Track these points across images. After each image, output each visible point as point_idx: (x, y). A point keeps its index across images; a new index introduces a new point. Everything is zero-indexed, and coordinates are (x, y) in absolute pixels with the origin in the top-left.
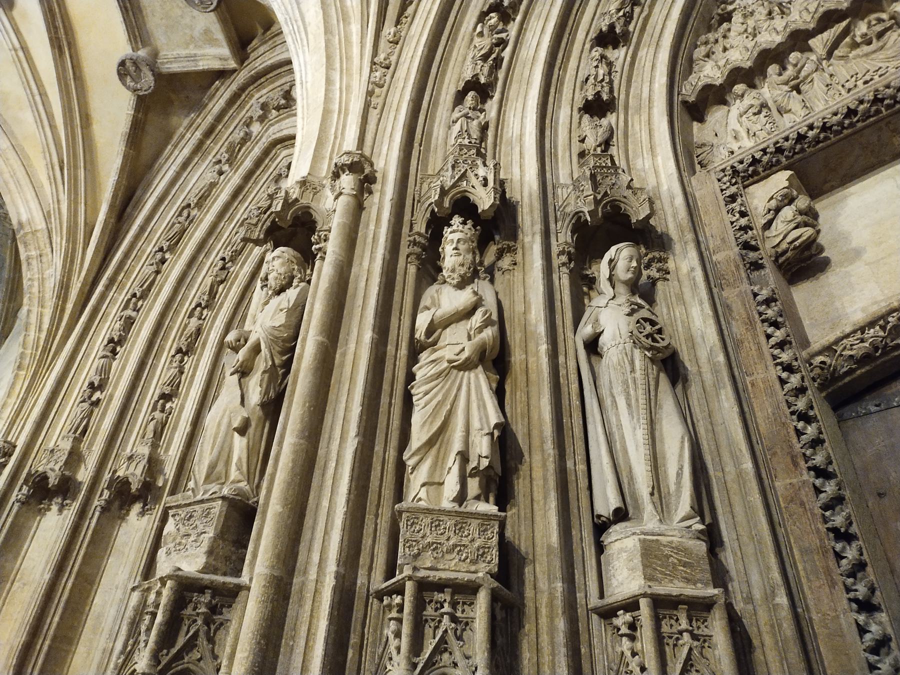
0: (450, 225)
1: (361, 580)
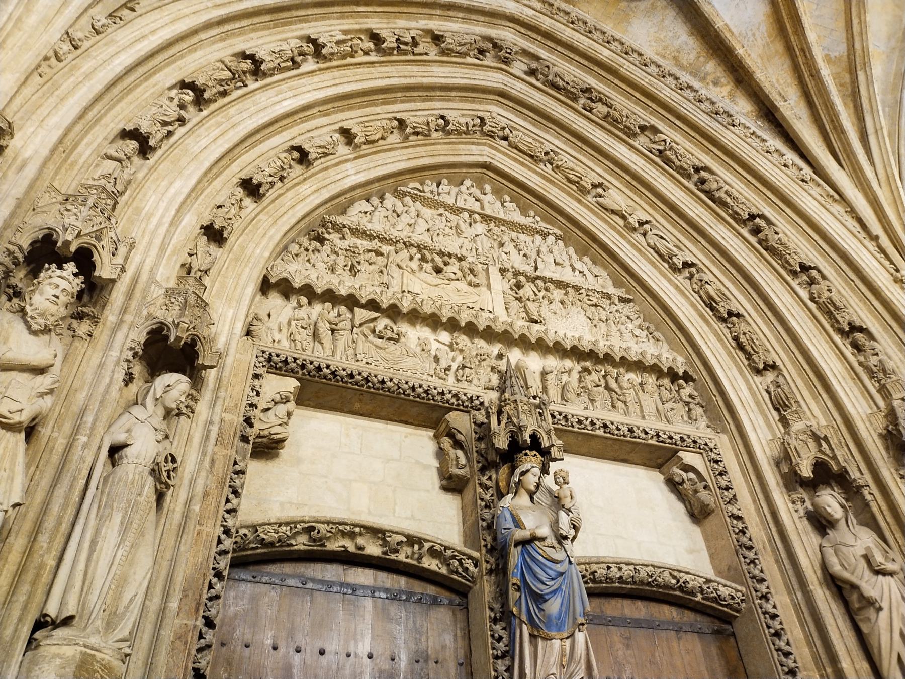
0: (60, 267)
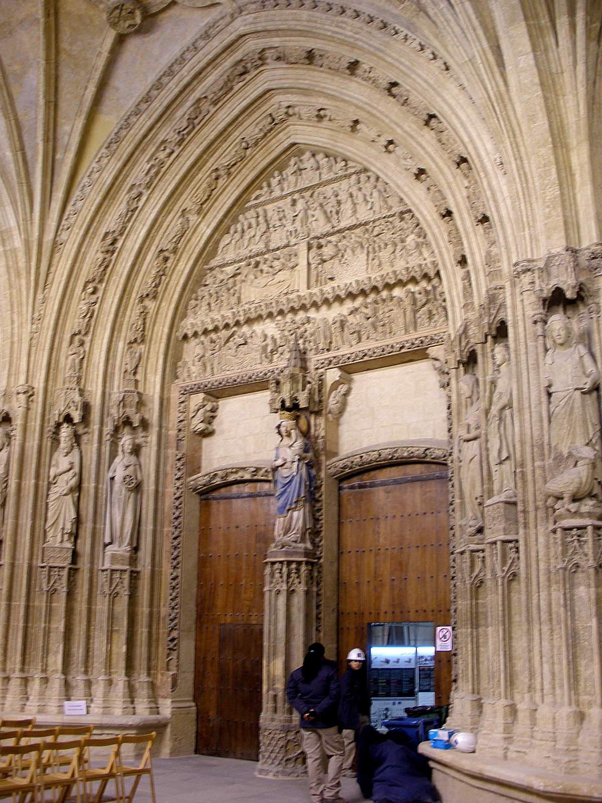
1: (34, 562)
